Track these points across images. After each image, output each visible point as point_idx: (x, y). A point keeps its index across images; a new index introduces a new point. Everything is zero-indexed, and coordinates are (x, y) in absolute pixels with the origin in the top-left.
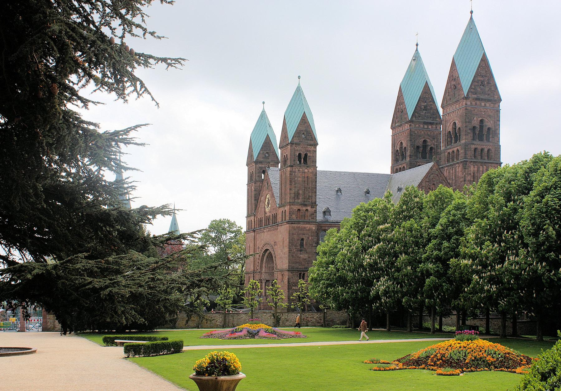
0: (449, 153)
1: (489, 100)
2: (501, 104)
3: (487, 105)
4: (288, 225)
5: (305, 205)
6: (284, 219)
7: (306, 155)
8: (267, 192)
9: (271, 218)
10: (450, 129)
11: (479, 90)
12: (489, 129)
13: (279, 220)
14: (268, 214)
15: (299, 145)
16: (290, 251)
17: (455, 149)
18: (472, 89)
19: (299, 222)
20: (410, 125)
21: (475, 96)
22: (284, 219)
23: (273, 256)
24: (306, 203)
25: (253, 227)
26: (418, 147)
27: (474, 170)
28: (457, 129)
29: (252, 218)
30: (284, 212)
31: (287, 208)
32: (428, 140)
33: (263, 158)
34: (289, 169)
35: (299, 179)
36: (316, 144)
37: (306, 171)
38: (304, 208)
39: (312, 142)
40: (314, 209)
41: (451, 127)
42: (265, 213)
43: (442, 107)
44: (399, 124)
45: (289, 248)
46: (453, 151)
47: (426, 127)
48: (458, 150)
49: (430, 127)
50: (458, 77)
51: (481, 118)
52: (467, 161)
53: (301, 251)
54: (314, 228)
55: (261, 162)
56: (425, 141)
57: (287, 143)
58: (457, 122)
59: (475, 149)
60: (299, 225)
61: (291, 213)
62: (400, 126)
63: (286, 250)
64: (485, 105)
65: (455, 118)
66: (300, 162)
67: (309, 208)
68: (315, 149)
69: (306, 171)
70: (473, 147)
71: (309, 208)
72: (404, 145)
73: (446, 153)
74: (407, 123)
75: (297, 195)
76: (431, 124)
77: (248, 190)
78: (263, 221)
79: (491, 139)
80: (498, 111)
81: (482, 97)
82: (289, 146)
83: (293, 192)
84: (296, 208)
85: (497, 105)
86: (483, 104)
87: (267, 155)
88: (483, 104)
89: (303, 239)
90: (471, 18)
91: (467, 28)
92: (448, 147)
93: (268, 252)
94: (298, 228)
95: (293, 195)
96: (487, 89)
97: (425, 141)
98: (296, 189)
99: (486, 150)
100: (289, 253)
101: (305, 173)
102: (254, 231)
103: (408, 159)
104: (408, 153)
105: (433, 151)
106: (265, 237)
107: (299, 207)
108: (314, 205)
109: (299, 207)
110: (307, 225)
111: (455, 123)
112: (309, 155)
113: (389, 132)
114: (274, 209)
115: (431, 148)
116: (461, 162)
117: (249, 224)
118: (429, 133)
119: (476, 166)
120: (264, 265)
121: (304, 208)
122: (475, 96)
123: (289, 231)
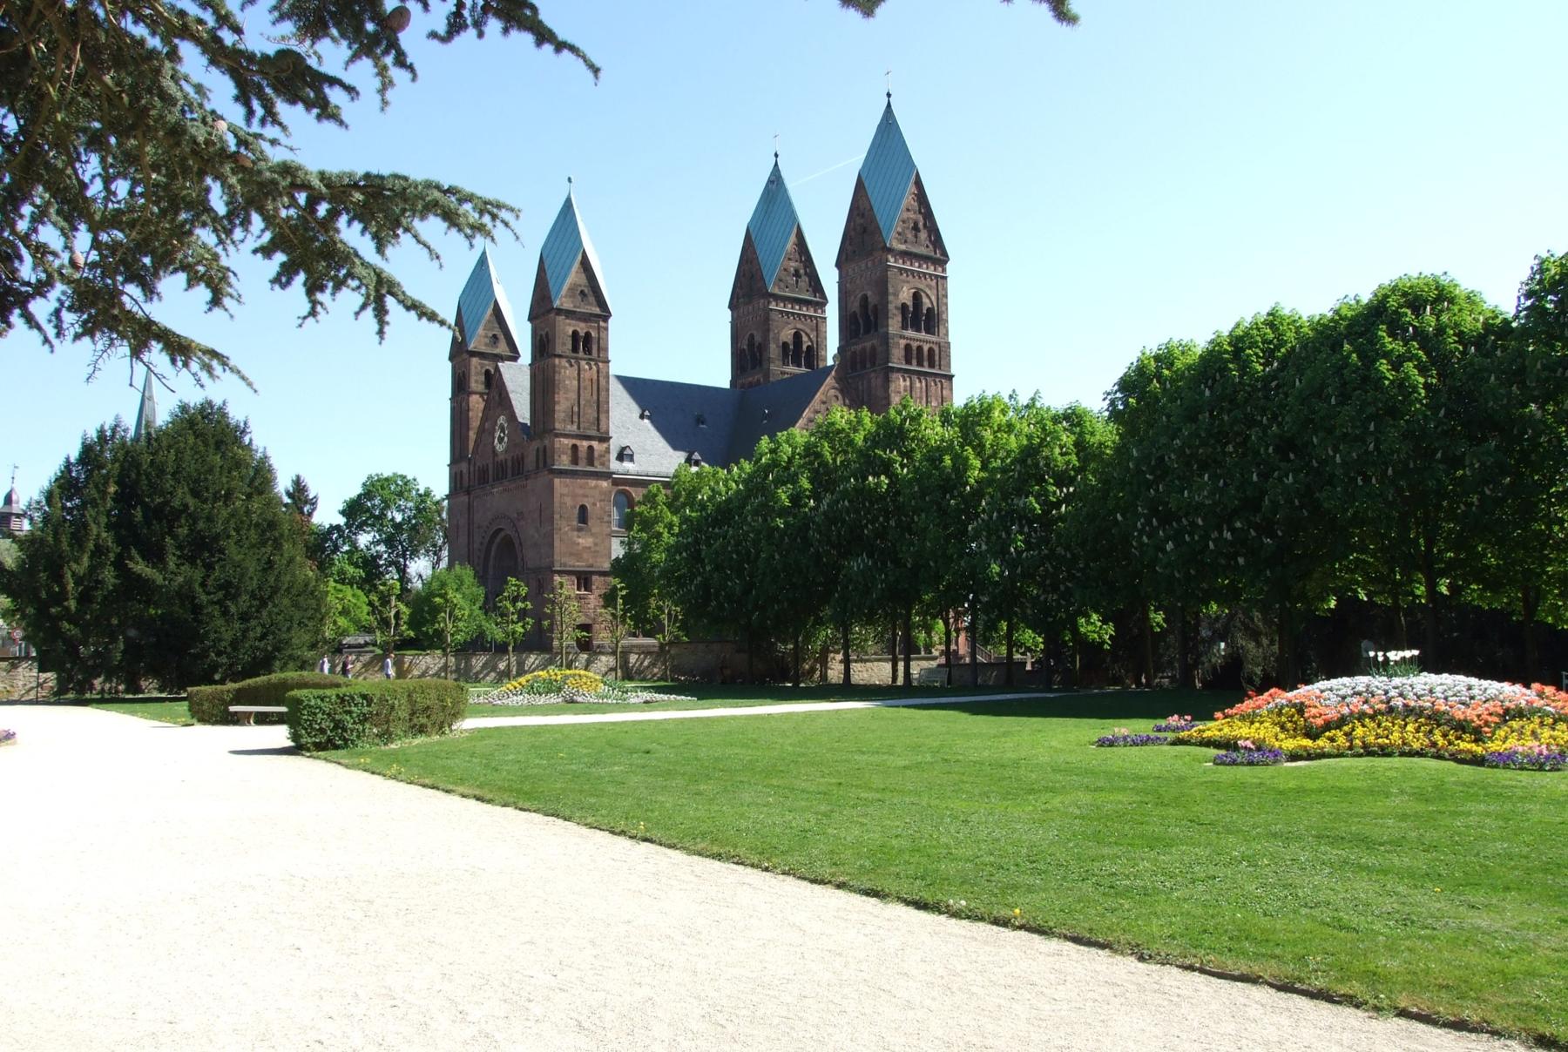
14: (501, 457)
17: (868, 345)
21: (903, 247)
23: (516, 542)
25: (466, 484)
29: (464, 466)
41: (857, 304)
46: (864, 349)
53: (579, 530)
76: (807, 303)
77: (453, 409)
90: (889, 105)
93: (502, 534)
98: (568, 404)
99: (926, 348)
102: (468, 493)
108: (605, 439)
111: (865, 298)
113: (727, 315)
120: (491, 563)
121: (585, 443)
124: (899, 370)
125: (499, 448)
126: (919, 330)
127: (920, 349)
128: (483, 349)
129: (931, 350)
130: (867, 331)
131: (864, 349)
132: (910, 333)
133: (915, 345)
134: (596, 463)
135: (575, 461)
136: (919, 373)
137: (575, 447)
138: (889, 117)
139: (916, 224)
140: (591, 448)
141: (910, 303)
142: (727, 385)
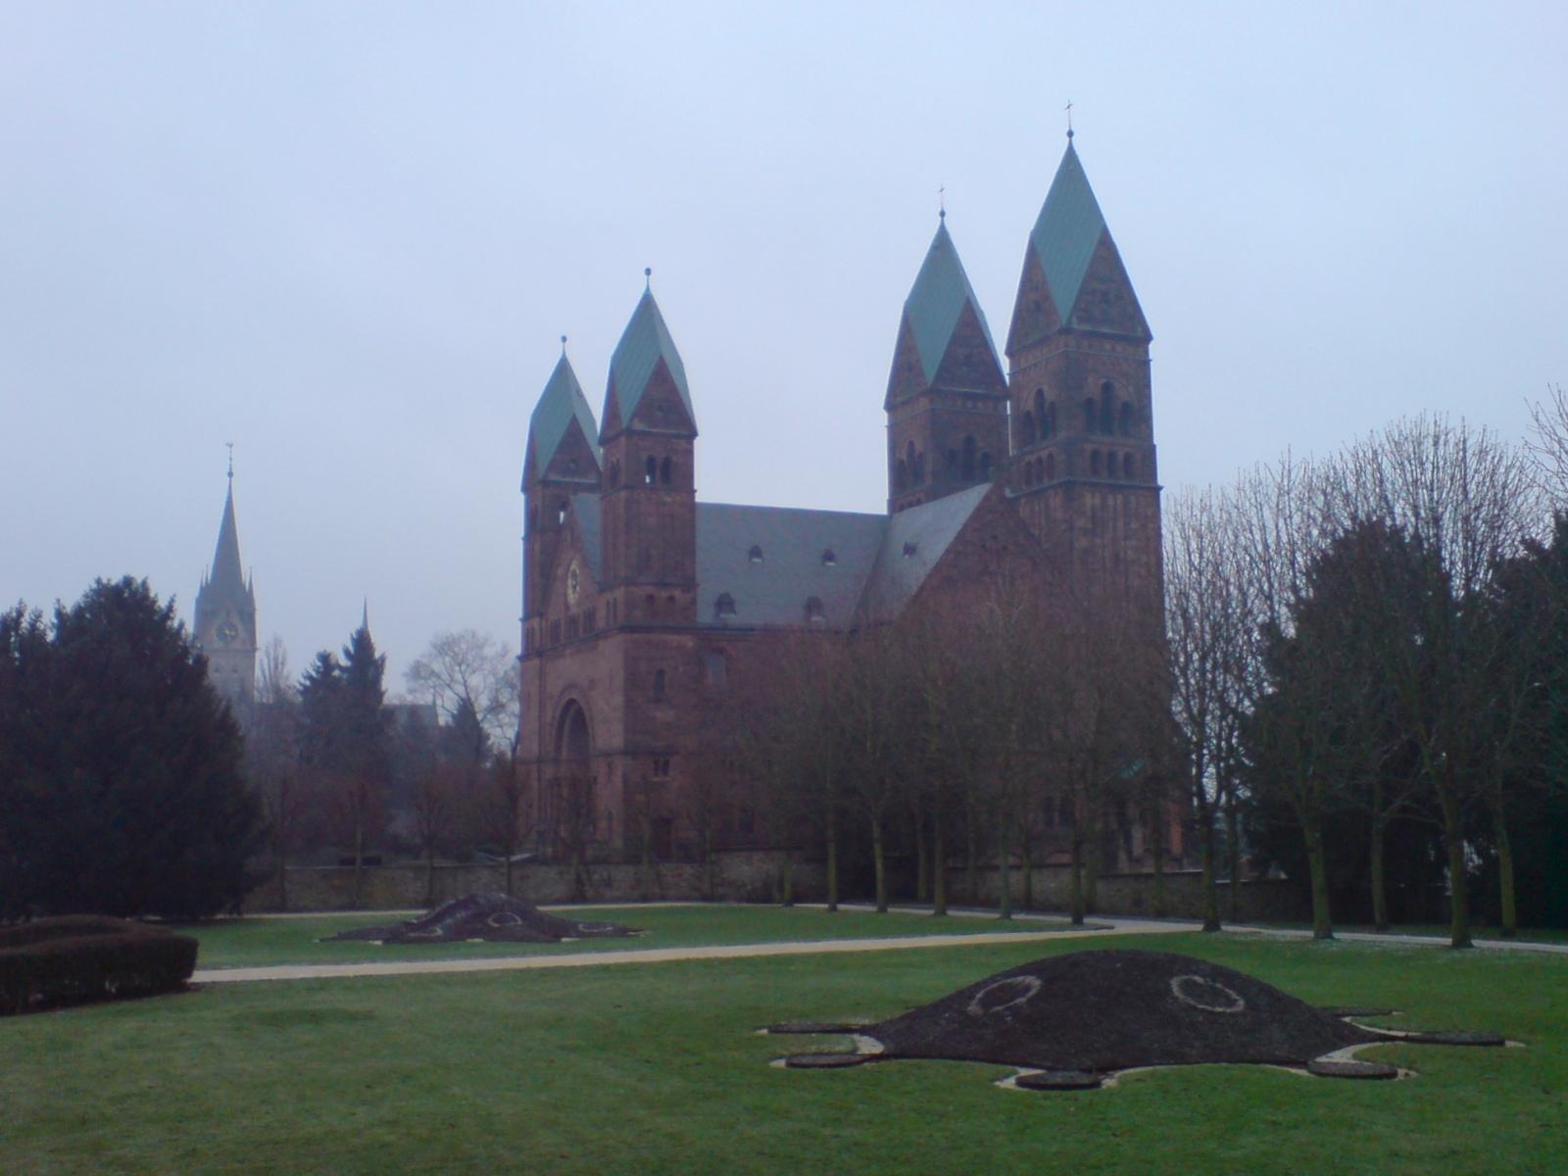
0: (1029, 464)
1: (1123, 339)
2: (1151, 346)
3: (1119, 348)
10: (1029, 404)
12: (1126, 405)
13: (601, 623)
14: (574, 610)
17: (1044, 454)
18: (1082, 310)
19: (649, 629)
21: (1087, 327)
31: (619, 594)
34: (623, 494)
36: (692, 433)
37: (668, 499)
38: (664, 594)
42: (567, 607)
43: (1010, 353)
46: (1040, 461)
49: (980, 404)
51: (1104, 380)
56: (970, 440)
58: (1045, 388)
59: (1095, 454)
63: (618, 700)
67: (677, 593)
69: (668, 499)
70: (1088, 447)
71: (677, 593)
72: (919, 447)
73: (1023, 464)
78: (563, 628)
80: (1145, 364)
82: (623, 440)
87: (572, 466)
88: (1108, 346)
89: (661, 673)
92: (1026, 449)
97: (970, 440)
104: (929, 467)
106: (569, 668)
107: (649, 590)
108: (690, 585)
111: (1040, 393)
112: (674, 459)
116: (1060, 485)
117: (528, 636)
121: (664, 594)
127: (1112, 456)
129: (1128, 458)
131: (1040, 461)
138: (1071, 157)
140: (671, 599)
142: (882, 509)
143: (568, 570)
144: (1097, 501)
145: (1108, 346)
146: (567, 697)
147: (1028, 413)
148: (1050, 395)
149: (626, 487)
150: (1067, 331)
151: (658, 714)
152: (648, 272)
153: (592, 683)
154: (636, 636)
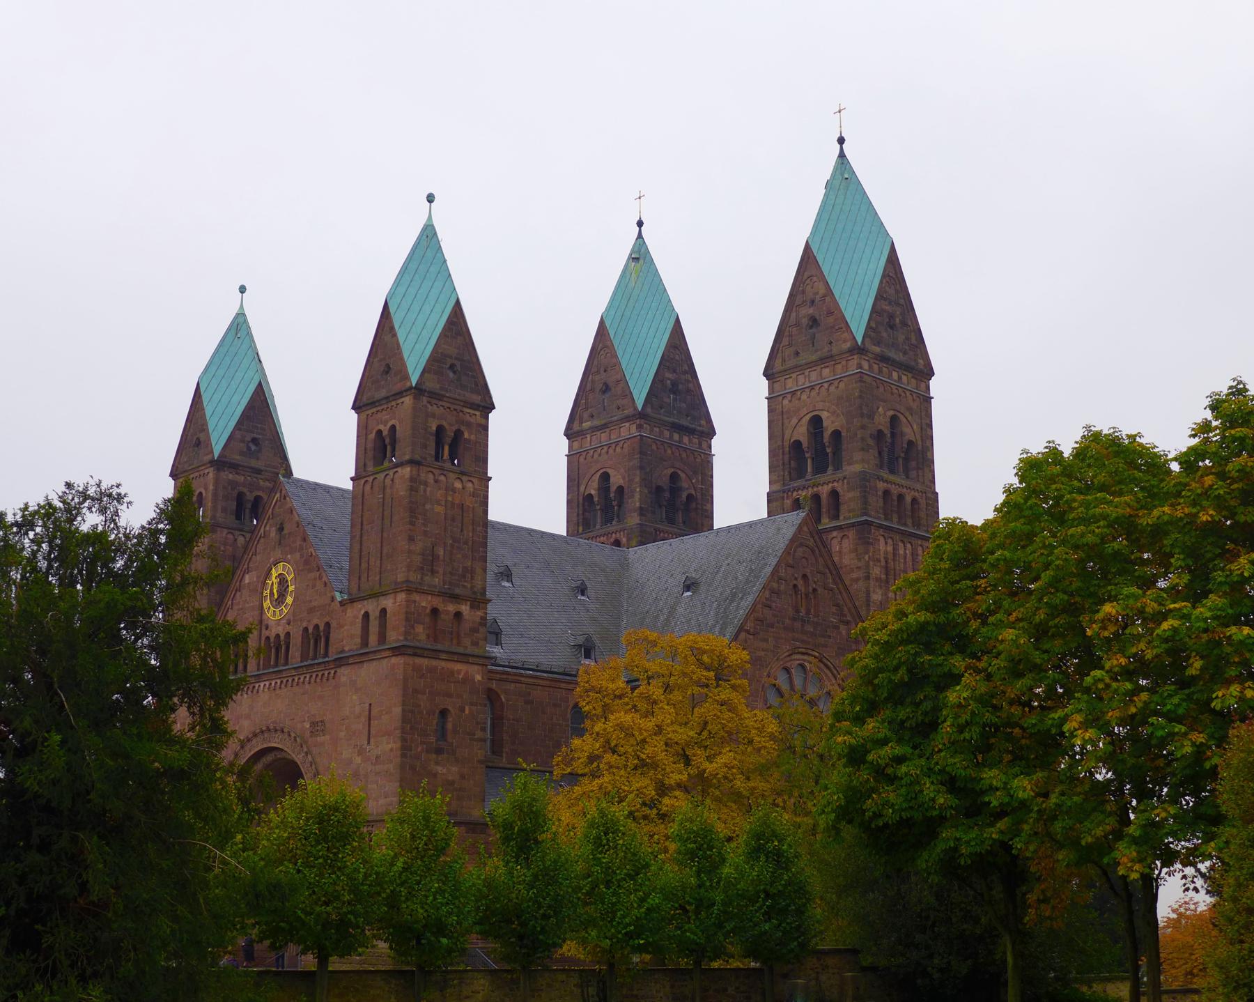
4: (398, 661)
5: (455, 598)
6: (373, 639)
7: (458, 433)
8: (278, 554)
9: (296, 640)
11: (885, 334)
12: (910, 443)
15: (440, 397)
16: (405, 749)
17: (824, 491)
19: (435, 654)
20: (640, 427)
21: (877, 350)
22: (373, 639)
24: (458, 591)
26: (659, 489)
27: (886, 553)
28: (827, 435)
30: (374, 614)
32: (682, 475)
33: (242, 453)
34: (406, 471)
35: (439, 509)
37: (458, 485)
39: (476, 399)
40: (480, 613)
44: (597, 422)
45: (404, 740)
47: (676, 436)
48: (834, 494)
49: (686, 439)
50: (829, 291)
51: (891, 413)
52: (869, 523)
53: (439, 751)
54: (478, 678)
55: (234, 467)
56: (674, 477)
57: (397, 388)
58: (824, 415)
59: (886, 493)
60: (434, 663)
61: (411, 619)
62: (603, 427)
63: (388, 746)
64: (900, 378)
65: (820, 406)
66: (437, 457)
67: (465, 609)
68: (483, 421)
69: (458, 485)
71: (465, 609)
72: (616, 480)
74: (627, 419)
75: (429, 562)
79: (913, 474)
81: (892, 354)
83: (418, 547)
84: (425, 602)
85: (923, 385)
86: (895, 375)
87: (253, 448)
89: (444, 713)
91: (833, 175)
92: (796, 484)
94: (432, 670)
95: (417, 559)
96: (901, 338)
97: (674, 477)
99: (908, 499)
100: (403, 755)
101: (454, 490)
103: (633, 520)
104: (635, 501)
105: (694, 505)
109: (437, 602)
110: (458, 666)
111: (816, 422)
112: (466, 435)
114: (311, 610)
115: (690, 497)
116: (853, 525)
118: (684, 455)
119: (890, 541)
121: (451, 608)
122: (877, 350)
123: (405, 680)
124: (880, 526)
125: (272, 614)
126: (892, 472)
127: (901, 497)
128: (237, 458)
129: (914, 500)
130: (820, 469)
132: (885, 474)
133: (895, 491)
134: (467, 642)
135: (435, 635)
136: (903, 533)
137: (435, 611)
139: (891, 317)
140: (458, 615)
141: (887, 432)
143: (268, 574)
144: (890, 549)
145: (895, 375)
146: (257, 746)
147: (797, 444)
148: (830, 423)
149: (412, 462)
150: (858, 350)
151: (440, 769)
152: (430, 199)
153: (318, 726)
154: (418, 660)
